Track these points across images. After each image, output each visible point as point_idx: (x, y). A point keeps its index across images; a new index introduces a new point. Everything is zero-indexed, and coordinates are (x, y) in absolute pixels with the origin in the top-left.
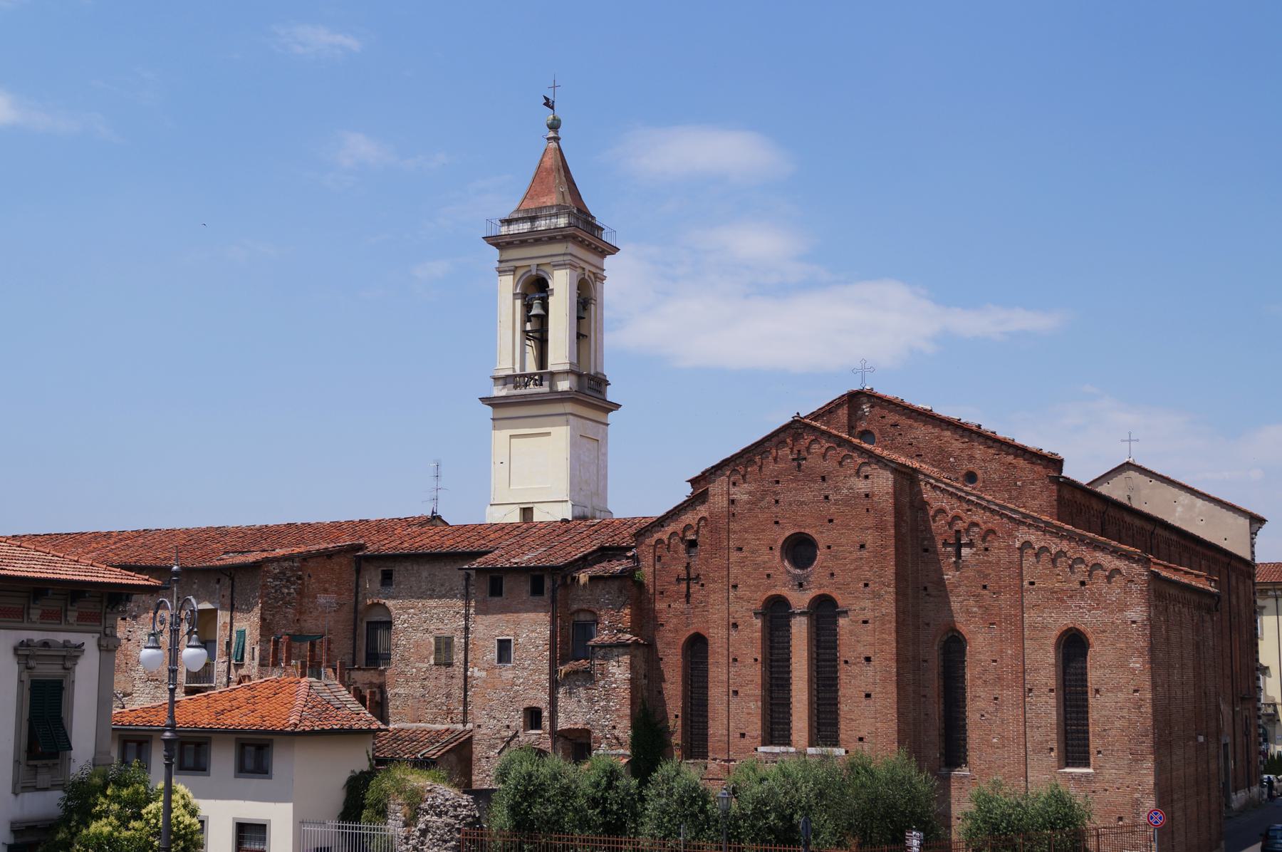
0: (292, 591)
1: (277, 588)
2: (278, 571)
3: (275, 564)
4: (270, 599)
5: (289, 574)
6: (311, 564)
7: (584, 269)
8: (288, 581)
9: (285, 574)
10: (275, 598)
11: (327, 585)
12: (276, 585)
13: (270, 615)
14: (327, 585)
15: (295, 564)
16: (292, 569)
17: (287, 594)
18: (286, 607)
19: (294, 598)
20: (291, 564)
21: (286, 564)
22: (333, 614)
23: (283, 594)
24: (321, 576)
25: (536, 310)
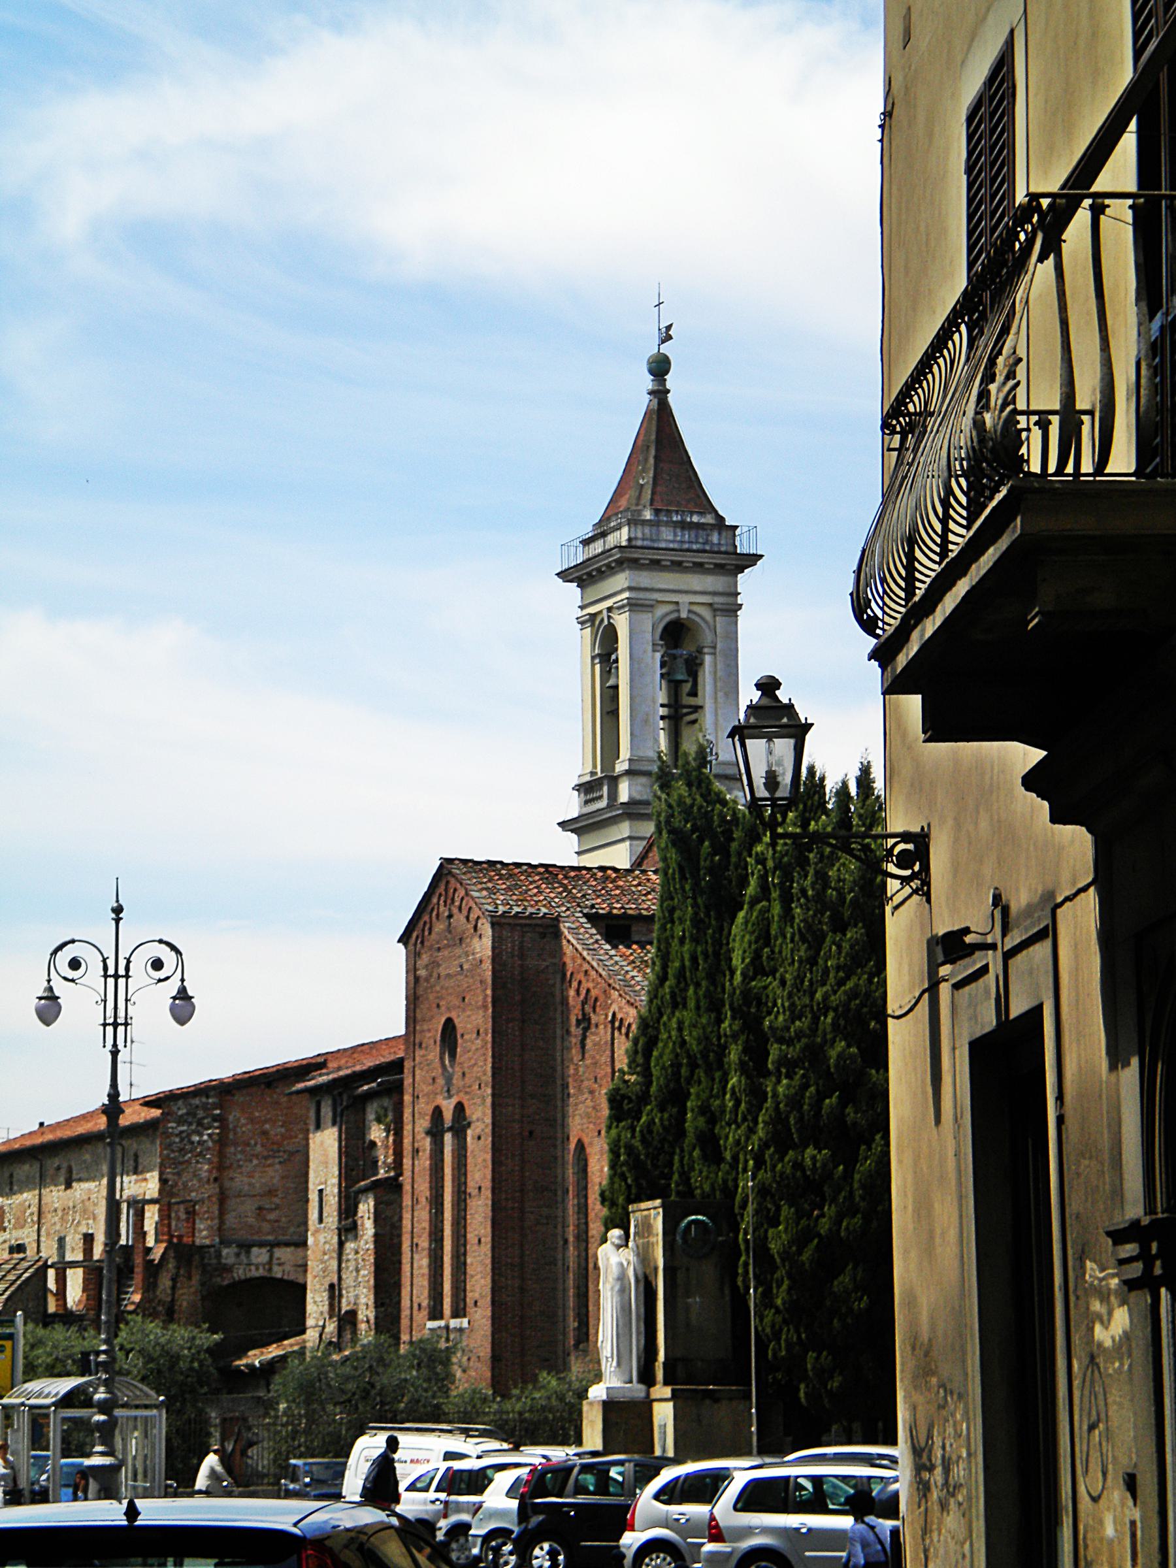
0: (205, 1137)
1: (184, 1135)
2: (184, 1111)
3: (180, 1103)
4: (173, 1151)
5: (201, 1114)
6: (239, 1098)
7: (677, 603)
8: (200, 1123)
9: (194, 1115)
10: (181, 1150)
11: (267, 1126)
12: (182, 1132)
13: (174, 1174)
14: (267, 1126)
15: (210, 1101)
16: (205, 1107)
17: (199, 1142)
18: (198, 1162)
19: (208, 1149)
20: (204, 1100)
21: (196, 1101)
22: (278, 1167)
23: (192, 1143)
24: (257, 1114)
25: (611, 683)
